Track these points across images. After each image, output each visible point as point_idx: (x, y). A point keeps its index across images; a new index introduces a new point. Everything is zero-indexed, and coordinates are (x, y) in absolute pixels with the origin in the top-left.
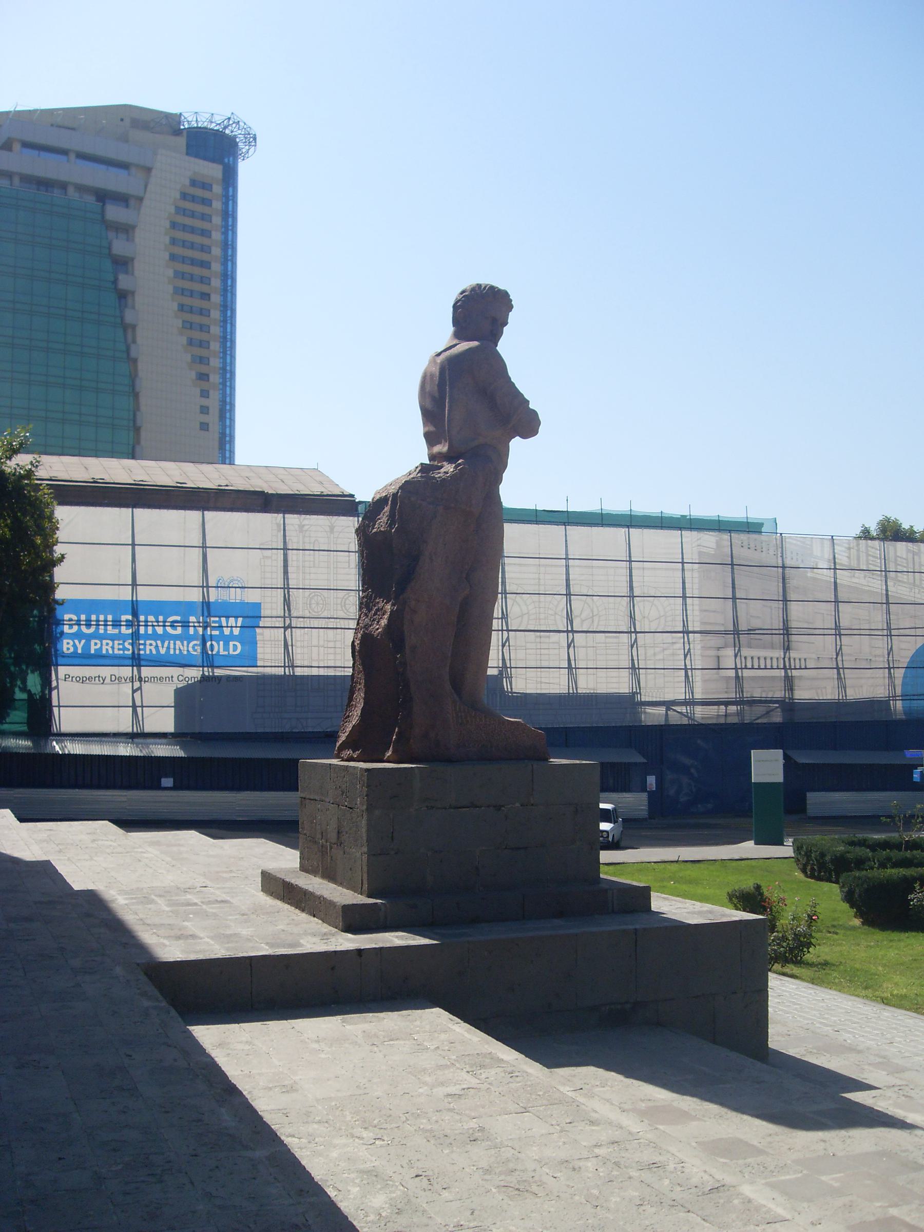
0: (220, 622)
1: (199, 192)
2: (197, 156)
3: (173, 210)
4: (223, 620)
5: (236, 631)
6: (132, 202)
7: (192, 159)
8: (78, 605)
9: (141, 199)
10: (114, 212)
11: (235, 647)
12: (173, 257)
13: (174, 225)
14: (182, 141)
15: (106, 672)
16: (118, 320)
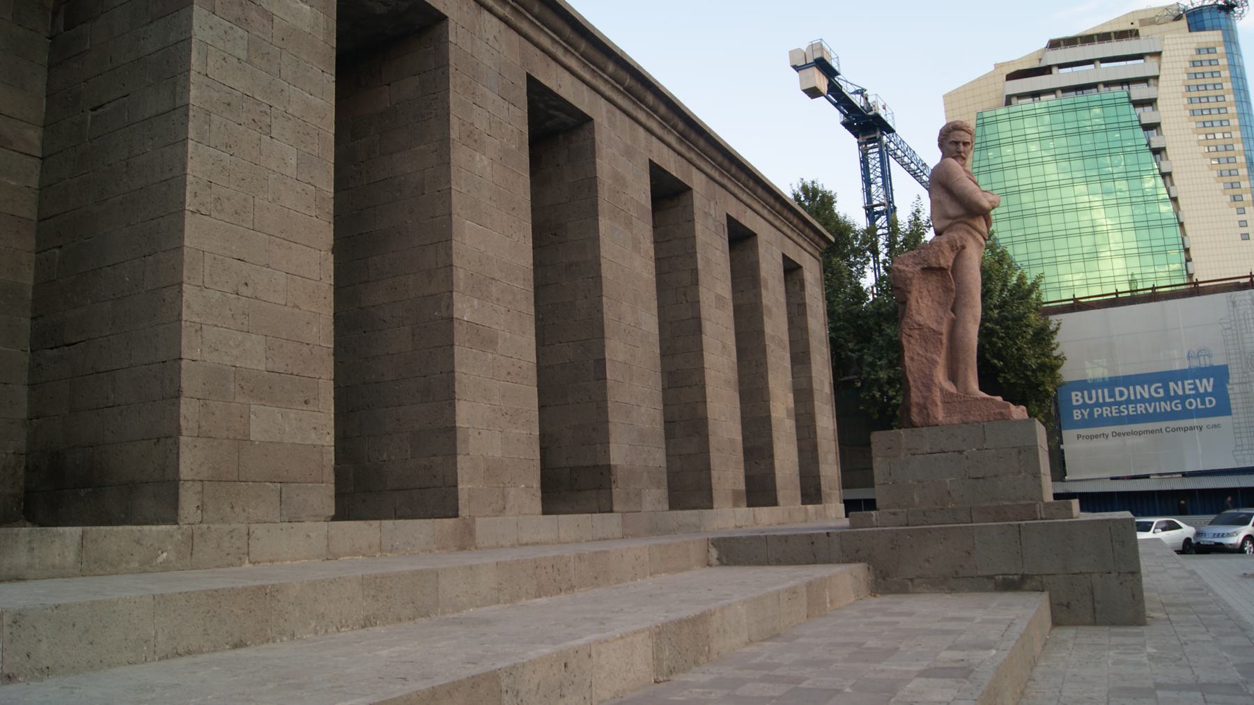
0: (1194, 384)
1: (1205, 57)
2: (1198, 30)
3: (1185, 77)
4: (1197, 381)
5: (1210, 390)
6: (1151, 81)
7: (1194, 34)
8: (1083, 385)
9: (1157, 78)
10: (1139, 92)
11: (1211, 402)
12: (1193, 112)
13: (1189, 88)
14: (1183, 23)
15: (1108, 430)
16: (1157, 172)
